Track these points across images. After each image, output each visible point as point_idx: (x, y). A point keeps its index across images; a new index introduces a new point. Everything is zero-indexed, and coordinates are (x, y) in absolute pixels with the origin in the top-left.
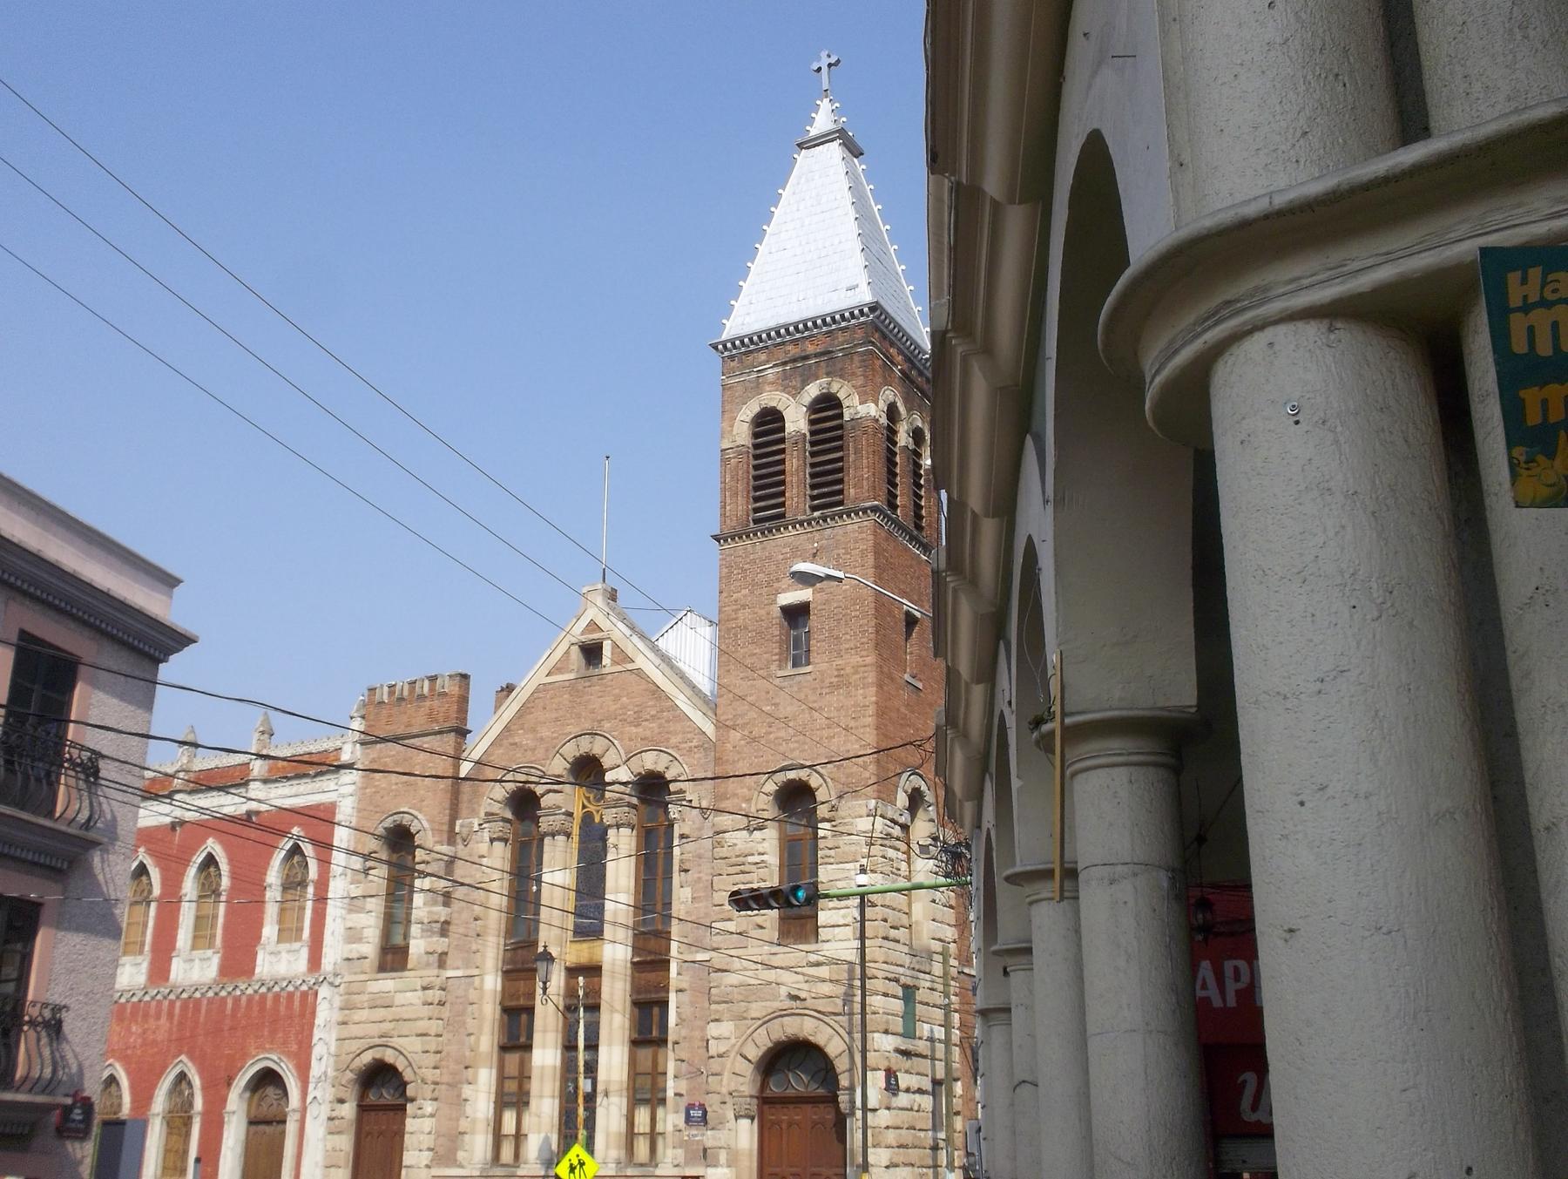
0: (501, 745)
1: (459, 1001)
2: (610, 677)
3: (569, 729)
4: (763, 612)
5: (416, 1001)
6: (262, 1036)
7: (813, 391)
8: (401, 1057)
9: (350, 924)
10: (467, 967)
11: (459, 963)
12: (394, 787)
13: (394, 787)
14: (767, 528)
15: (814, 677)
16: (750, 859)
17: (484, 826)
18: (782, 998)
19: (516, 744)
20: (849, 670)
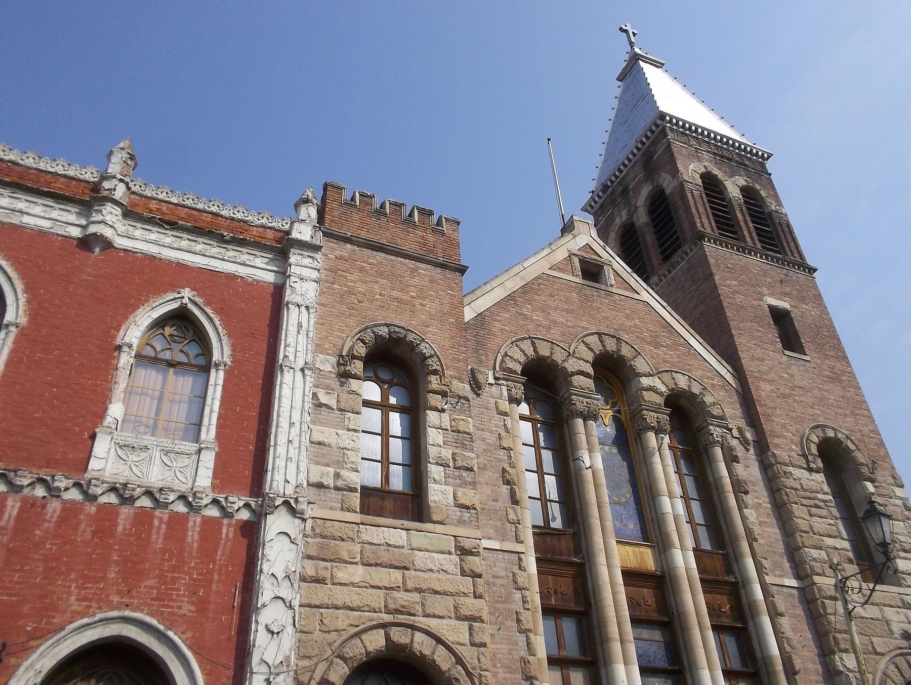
0: (508, 311)
1: (499, 582)
2: (617, 297)
3: (584, 324)
4: (754, 303)
5: (450, 568)
6: (104, 578)
7: (742, 181)
8: (441, 649)
9: (317, 437)
10: (503, 538)
11: (492, 532)
12: (378, 297)
13: (378, 297)
14: (742, 248)
15: (813, 365)
16: (820, 496)
17: (501, 382)
18: (896, 636)
19: (525, 315)
20: (836, 370)
